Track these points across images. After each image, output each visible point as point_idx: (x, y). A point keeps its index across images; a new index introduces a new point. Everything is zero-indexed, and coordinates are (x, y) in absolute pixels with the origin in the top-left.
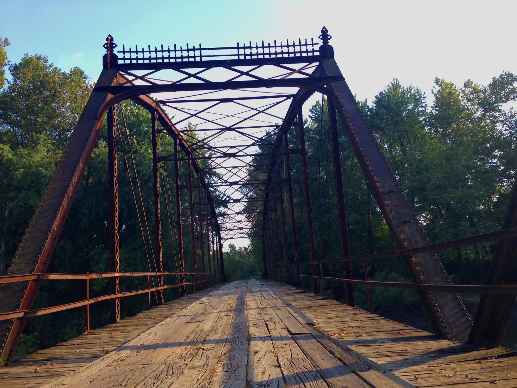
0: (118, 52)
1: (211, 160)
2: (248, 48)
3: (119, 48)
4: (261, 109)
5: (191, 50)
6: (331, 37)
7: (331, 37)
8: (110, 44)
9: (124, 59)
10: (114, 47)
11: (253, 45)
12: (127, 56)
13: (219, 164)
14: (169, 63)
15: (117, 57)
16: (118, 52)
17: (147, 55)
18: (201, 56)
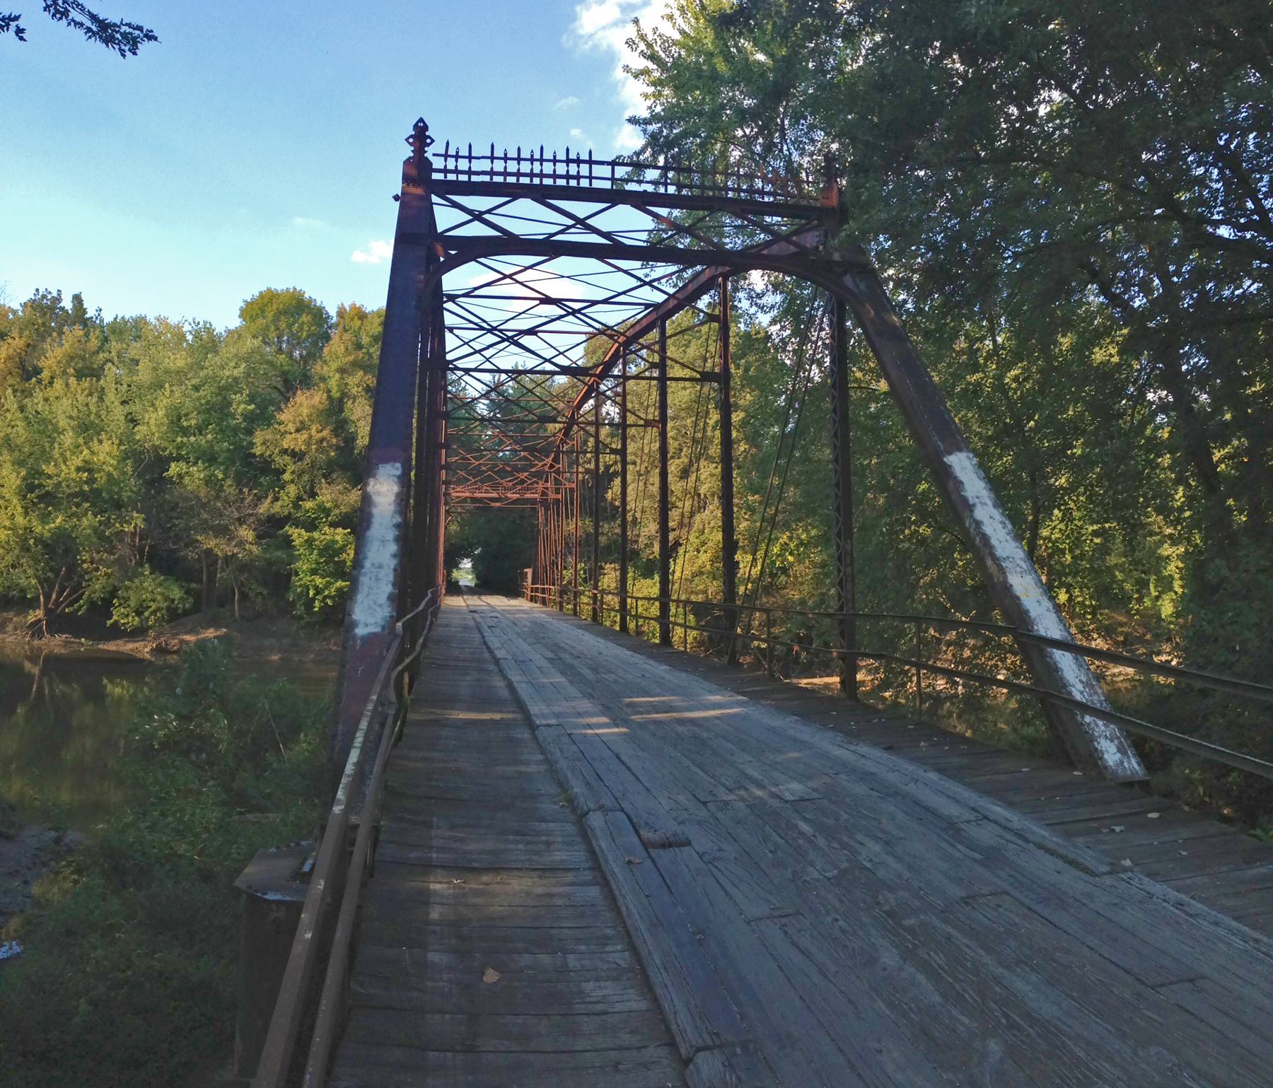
0: (434, 155)
1: (639, 344)
2: (584, 162)
3: (437, 147)
4: (508, 281)
5: (573, 161)
6: (407, 140)
7: (407, 140)
8: (420, 136)
9: (445, 171)
10: (429, 145)
11: (548, 155)
12: (451, 164)
13: (562, 351)
14: (505, 184)
15: (431, 164)
16: (434, 155)
17: (512, 166)
18: (591, 178)
